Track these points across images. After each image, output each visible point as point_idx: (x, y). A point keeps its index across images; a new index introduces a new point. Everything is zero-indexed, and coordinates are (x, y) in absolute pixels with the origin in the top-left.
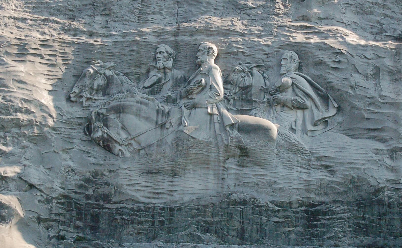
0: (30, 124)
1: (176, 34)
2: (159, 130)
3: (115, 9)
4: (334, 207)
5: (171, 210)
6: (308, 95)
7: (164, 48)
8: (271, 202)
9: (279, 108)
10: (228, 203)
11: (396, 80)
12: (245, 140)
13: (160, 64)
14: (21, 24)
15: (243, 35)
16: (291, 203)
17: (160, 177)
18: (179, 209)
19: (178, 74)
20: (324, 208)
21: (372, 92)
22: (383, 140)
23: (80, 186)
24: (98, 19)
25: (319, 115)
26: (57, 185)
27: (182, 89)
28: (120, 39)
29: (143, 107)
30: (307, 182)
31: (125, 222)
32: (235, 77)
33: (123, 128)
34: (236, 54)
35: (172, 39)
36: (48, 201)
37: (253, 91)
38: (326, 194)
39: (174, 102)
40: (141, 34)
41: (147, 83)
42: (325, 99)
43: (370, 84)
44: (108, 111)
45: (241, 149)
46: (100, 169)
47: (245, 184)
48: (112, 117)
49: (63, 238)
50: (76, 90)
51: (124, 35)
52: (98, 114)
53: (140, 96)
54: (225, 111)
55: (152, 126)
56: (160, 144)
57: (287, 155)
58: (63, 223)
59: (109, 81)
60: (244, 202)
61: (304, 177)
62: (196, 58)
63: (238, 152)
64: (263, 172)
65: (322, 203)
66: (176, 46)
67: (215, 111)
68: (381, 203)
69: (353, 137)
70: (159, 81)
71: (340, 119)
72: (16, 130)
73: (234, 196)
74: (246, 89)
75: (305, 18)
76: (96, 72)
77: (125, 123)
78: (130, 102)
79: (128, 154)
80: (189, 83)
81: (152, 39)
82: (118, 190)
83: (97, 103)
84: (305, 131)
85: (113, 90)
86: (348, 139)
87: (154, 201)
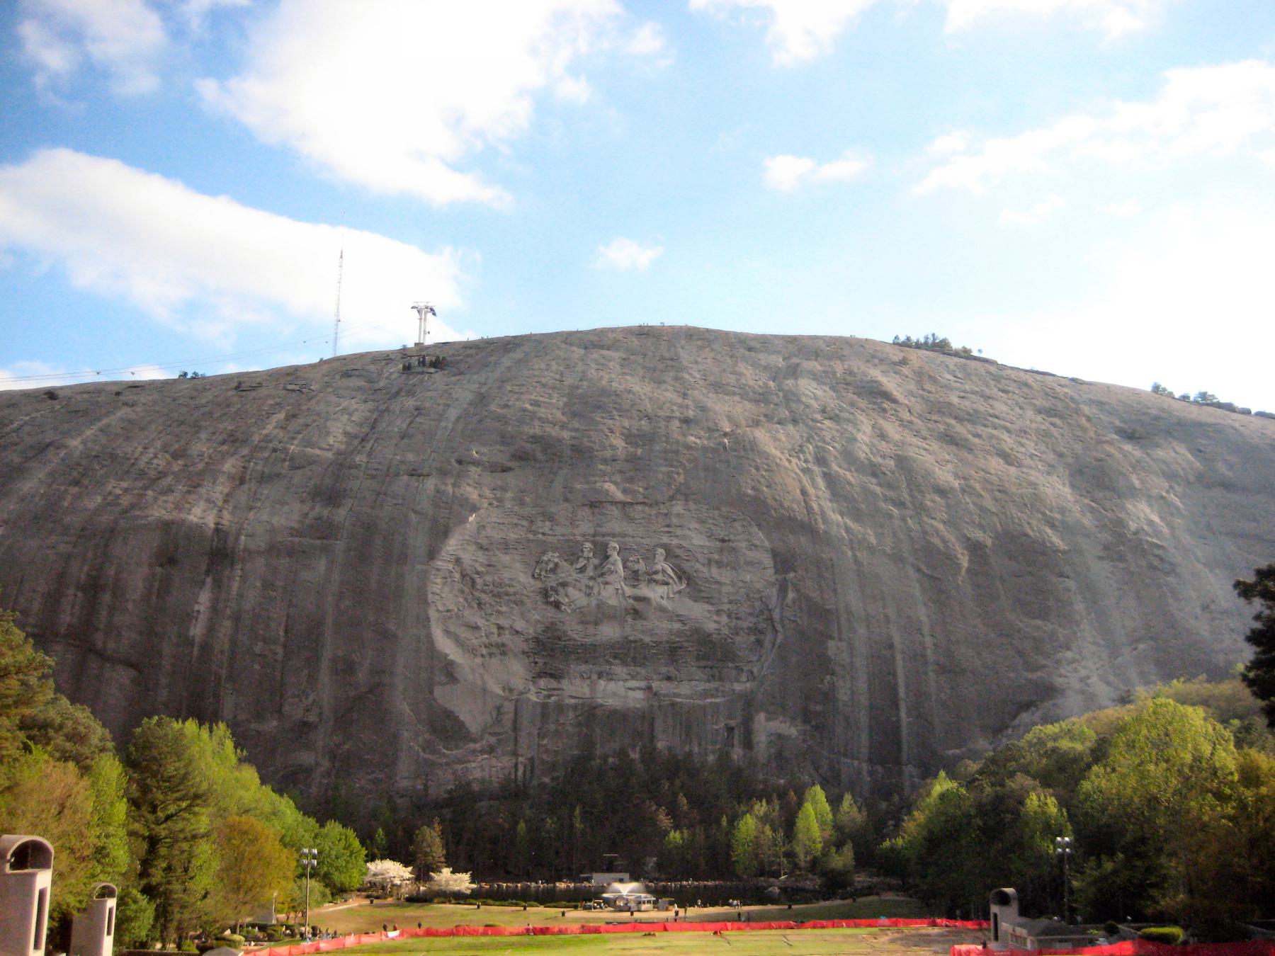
0: (515, 594)
1: (594, 536)
2: (587, 598)
3: (557, 517)
4: (685, 644)
5: (595, 645)
6: (672, 577)
7: (588, 545)
8: (651, 641)
9: (654, 584)
10: (627, 643)
11: (720, 567)
12: (638, 606)
13: (586, 554)
14: (501, 527)
15: (633, 537)
16: (661, 642)
17: (589, 626)
18: (600, 646)
19: (596, 561)
20: (679, 645)
21: (707, 575)
22: (712, 604)
23: (544, 631)
24: (547, 523)
25: (676, 588)
26: (531, 631)
27: (599, 572)
28: (562, 538)
29: (578, 583)
30: (671, 631)
31: (570, 652)
32: (630, 564)
33: (566, 595)
34: (630, 549)
35: (592, 539)
36: (527, 640)
37: (640, 572)
38: (680, 637)
39: (595, 579)
40: (574, 535)
41: (579, 565)
42: (680, 578)
43: (705, 570)
44: (557, 585)
45: (634, 610)
46: (554, 620)
47: (636, 630)
48: (560, 589)
49: (536, 663)
50: (538, 571)
51: (563, 535)
52: (552, 587)
53: (575, 576)
54: (626, 588)
55: (582, 595)
56: (588, 606)
57: (659, 613)
58: (536, 654)
59: (556, 565)
60: (635, 641)
61: (670, 627)
62: (607, 552)
63: (632, 611)
64: (645, 623)
65: (679, 642)
66: (594, 543)
67: (619, 587)
68: (711, 642)
69: (695, 601)
70: (585, 565)
71: (688, 590)
72: (507, 598)
73: (631, 638)
74: (636, 572)
75: (668, 526)
76: (549, 560)
77: (569, 594)
78: (569, 580)
79: (569, 611)
80: (603, 568)
81: (579, 538)
82: (564, 632)
83: (550, 579)
84: (668, 598)
85: (559, 571)
86: (693, 603)
87: (586, 640)
